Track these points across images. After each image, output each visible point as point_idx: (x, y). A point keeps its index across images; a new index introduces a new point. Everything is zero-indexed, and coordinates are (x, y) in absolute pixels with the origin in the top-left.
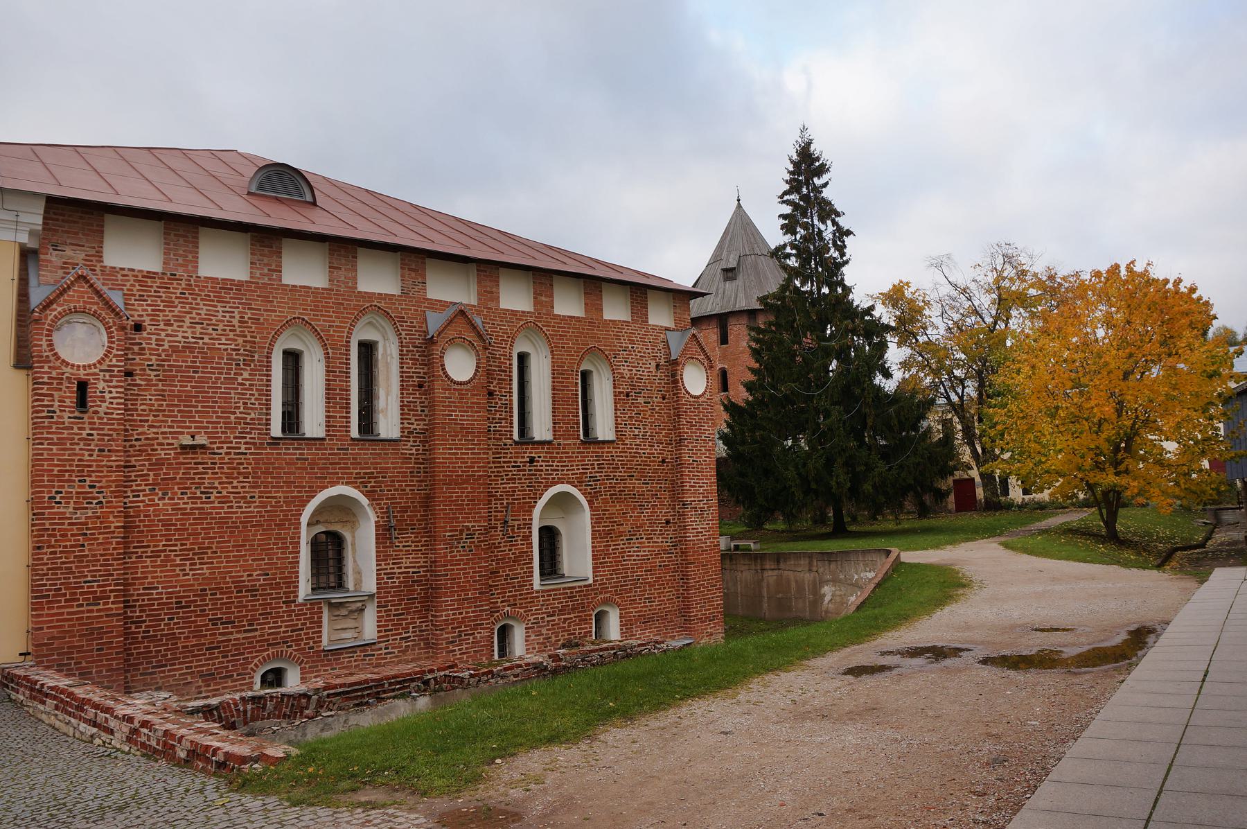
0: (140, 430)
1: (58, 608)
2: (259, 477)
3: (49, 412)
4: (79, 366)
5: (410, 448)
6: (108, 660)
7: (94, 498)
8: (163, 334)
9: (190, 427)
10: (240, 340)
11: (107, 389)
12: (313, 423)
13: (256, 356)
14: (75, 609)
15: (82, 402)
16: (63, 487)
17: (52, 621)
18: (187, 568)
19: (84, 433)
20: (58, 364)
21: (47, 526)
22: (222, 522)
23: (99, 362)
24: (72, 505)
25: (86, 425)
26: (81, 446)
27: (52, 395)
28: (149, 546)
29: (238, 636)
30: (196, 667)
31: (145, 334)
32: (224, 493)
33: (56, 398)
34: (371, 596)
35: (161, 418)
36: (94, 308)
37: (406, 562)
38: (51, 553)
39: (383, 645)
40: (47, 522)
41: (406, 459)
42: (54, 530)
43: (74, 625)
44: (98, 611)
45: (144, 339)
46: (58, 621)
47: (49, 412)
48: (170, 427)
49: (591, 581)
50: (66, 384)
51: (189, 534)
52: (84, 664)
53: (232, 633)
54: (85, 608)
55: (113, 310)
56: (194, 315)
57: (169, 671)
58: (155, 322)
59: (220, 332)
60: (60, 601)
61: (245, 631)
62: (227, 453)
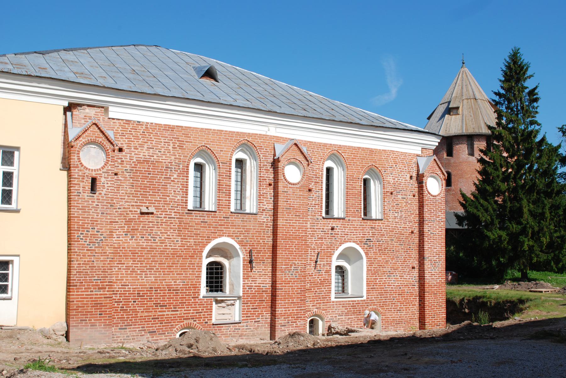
0: (121, 203)
1: (81, 292)
2: (181, 231)
3: (78, 193)
4: (92, 170)
6: (104, 320)
7: (99, 238)
8: (133, 153)
9: (146, 203)
10: (173, 157)
11: (106, 182)
12: (209, 204)
13: (181, 167)
14: (89, 293)
15: (93, 188)
16: (84, 231)
17: (78, 298)
18: (143, 276)
19: (95, 204)
20: (82, 168)
21: (76, 250)
22: (162, 253)
23: (102, 168)
24: (88, 241)
25: (96, 201)
26: (93, 210)
27: (79, 184)
28: (124, 264)
29: (168, 313)
30: (147, 327)
31: (124, 153)
32: (163, 238)
33: (81, 186)
34: (239, 298)
35: (131, 197)
36: (100, 140)
37: (259, 281)
38: (78, 264)
39: (245, 324)
40: (76, 249)
41: (261, 224)
42: (80, 252)
43: (89, 301)
44: (100, 295)
45: (124, 156)
46: (81, 298)
47: (78, 193)
48: (136, 202)
49: (365, 298)
50: (86, 179)
51: (144, 259)
52: (93, 321)
53: (165, 311)
54: (94, 293)
55: (110, 141)
56: (149, 144)
57: (133, 328)
58: (129, 147)
59: (162, 153)
60: (82, 289)
61: (172, 311)
62: (164, 217)
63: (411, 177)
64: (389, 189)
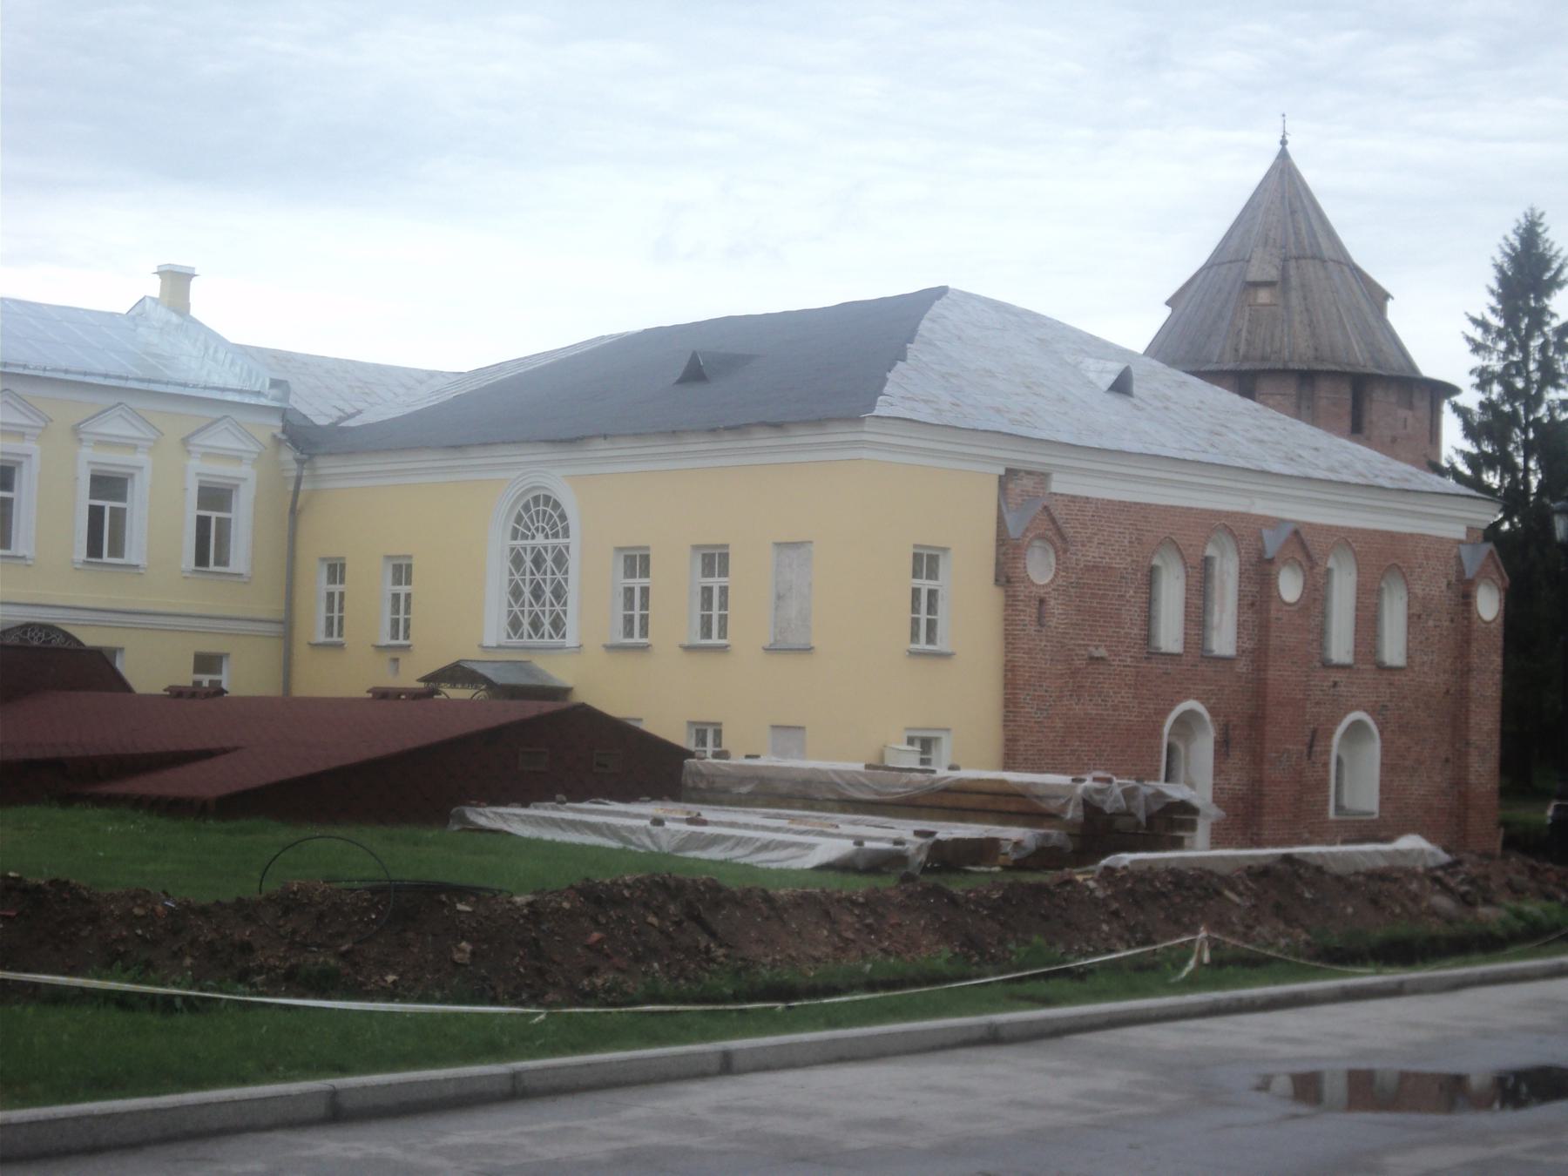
5: (1242, 667)
63: (1449, 584)
64: (1417, 609)
